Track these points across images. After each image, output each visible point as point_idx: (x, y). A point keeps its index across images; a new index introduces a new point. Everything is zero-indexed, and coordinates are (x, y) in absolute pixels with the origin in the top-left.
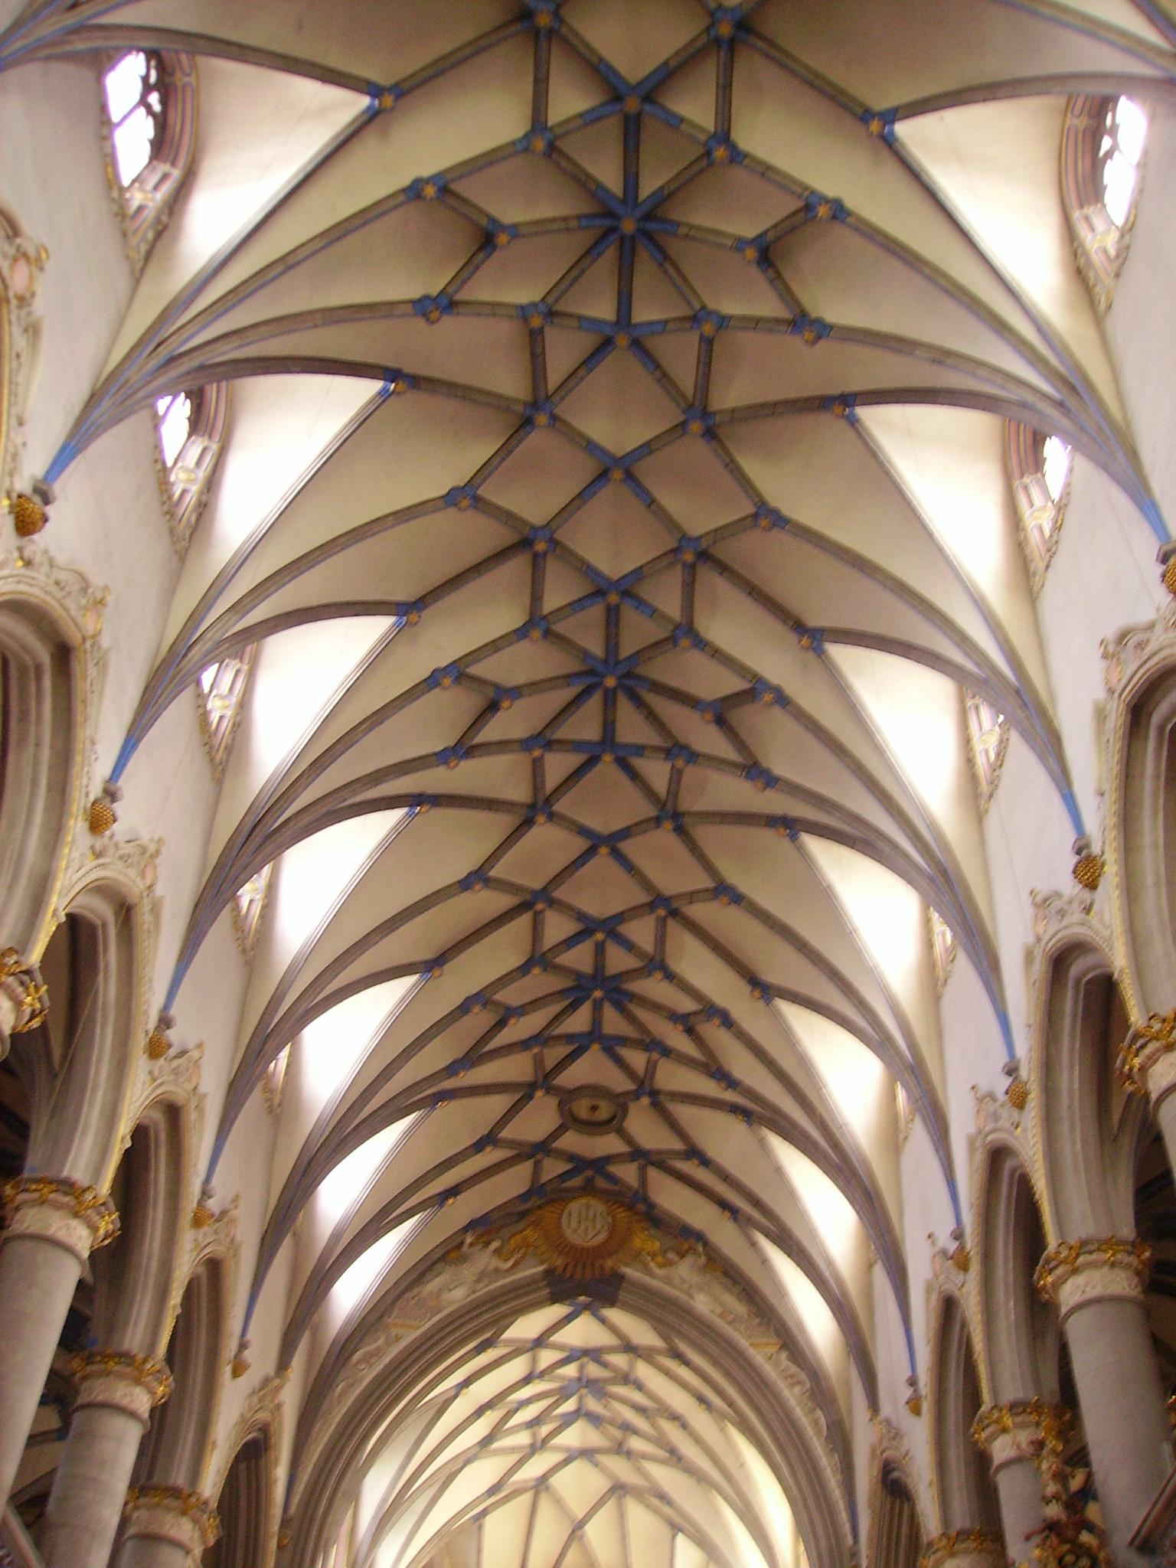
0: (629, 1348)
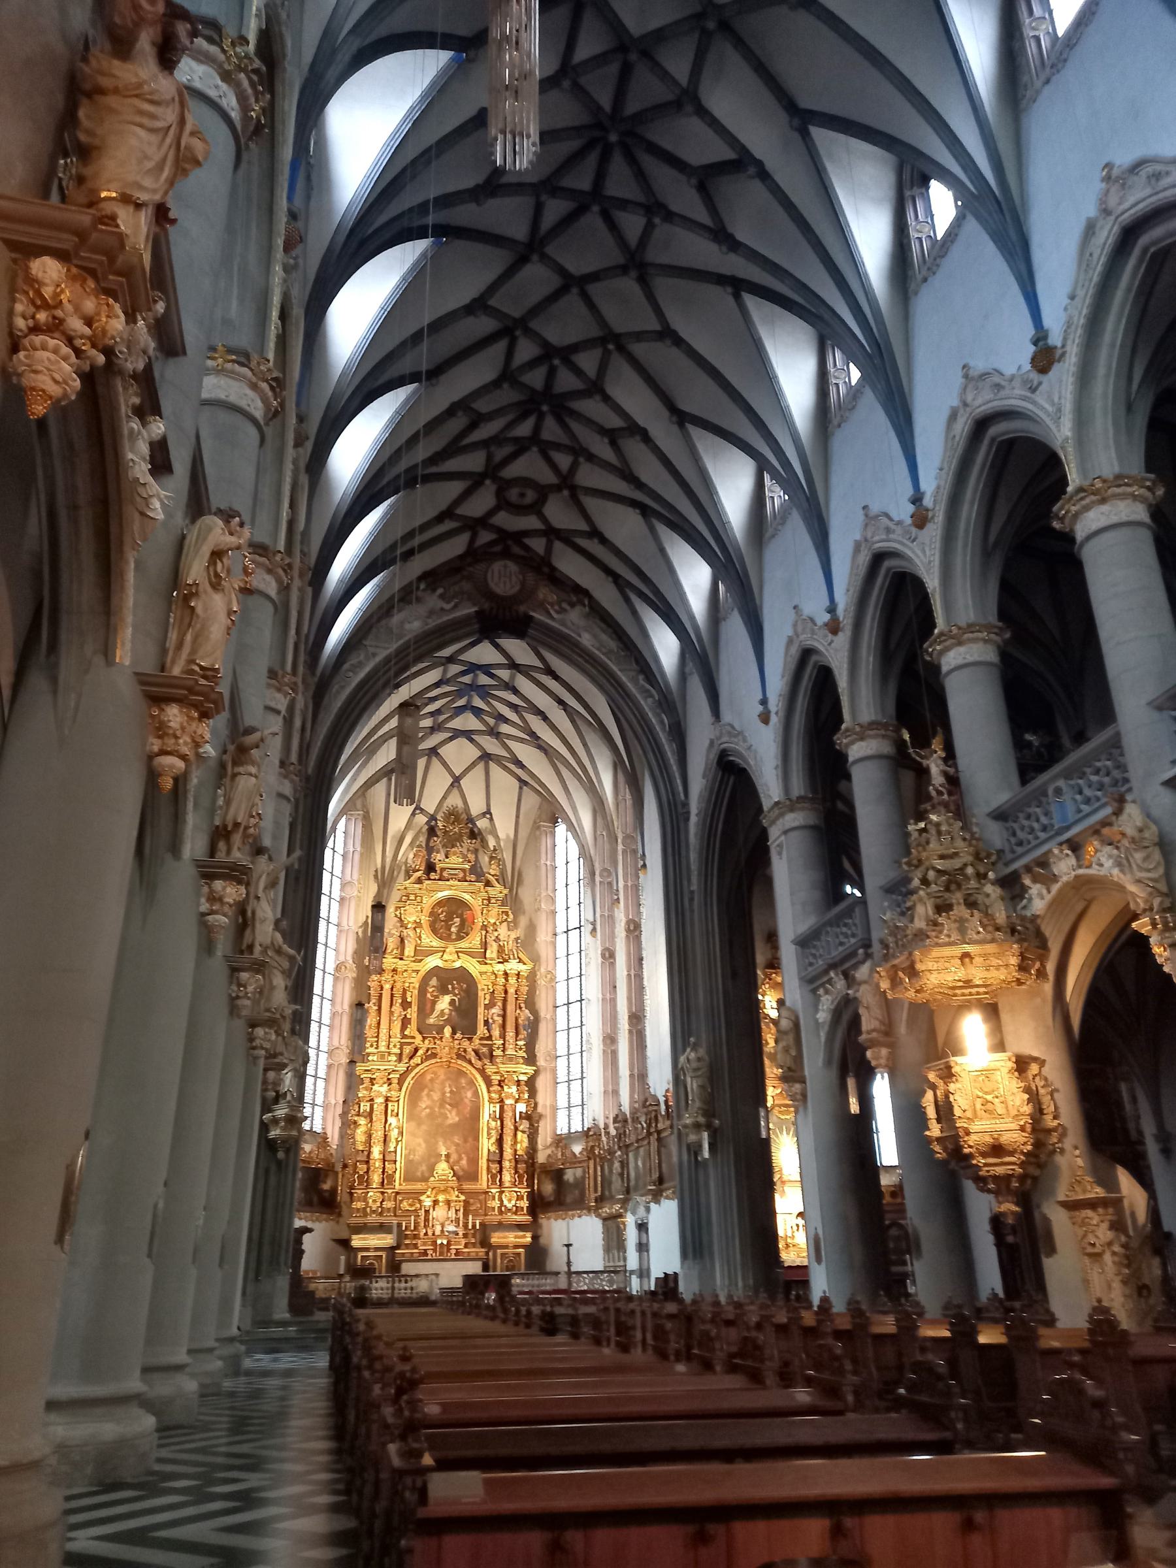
0: (514, 666)
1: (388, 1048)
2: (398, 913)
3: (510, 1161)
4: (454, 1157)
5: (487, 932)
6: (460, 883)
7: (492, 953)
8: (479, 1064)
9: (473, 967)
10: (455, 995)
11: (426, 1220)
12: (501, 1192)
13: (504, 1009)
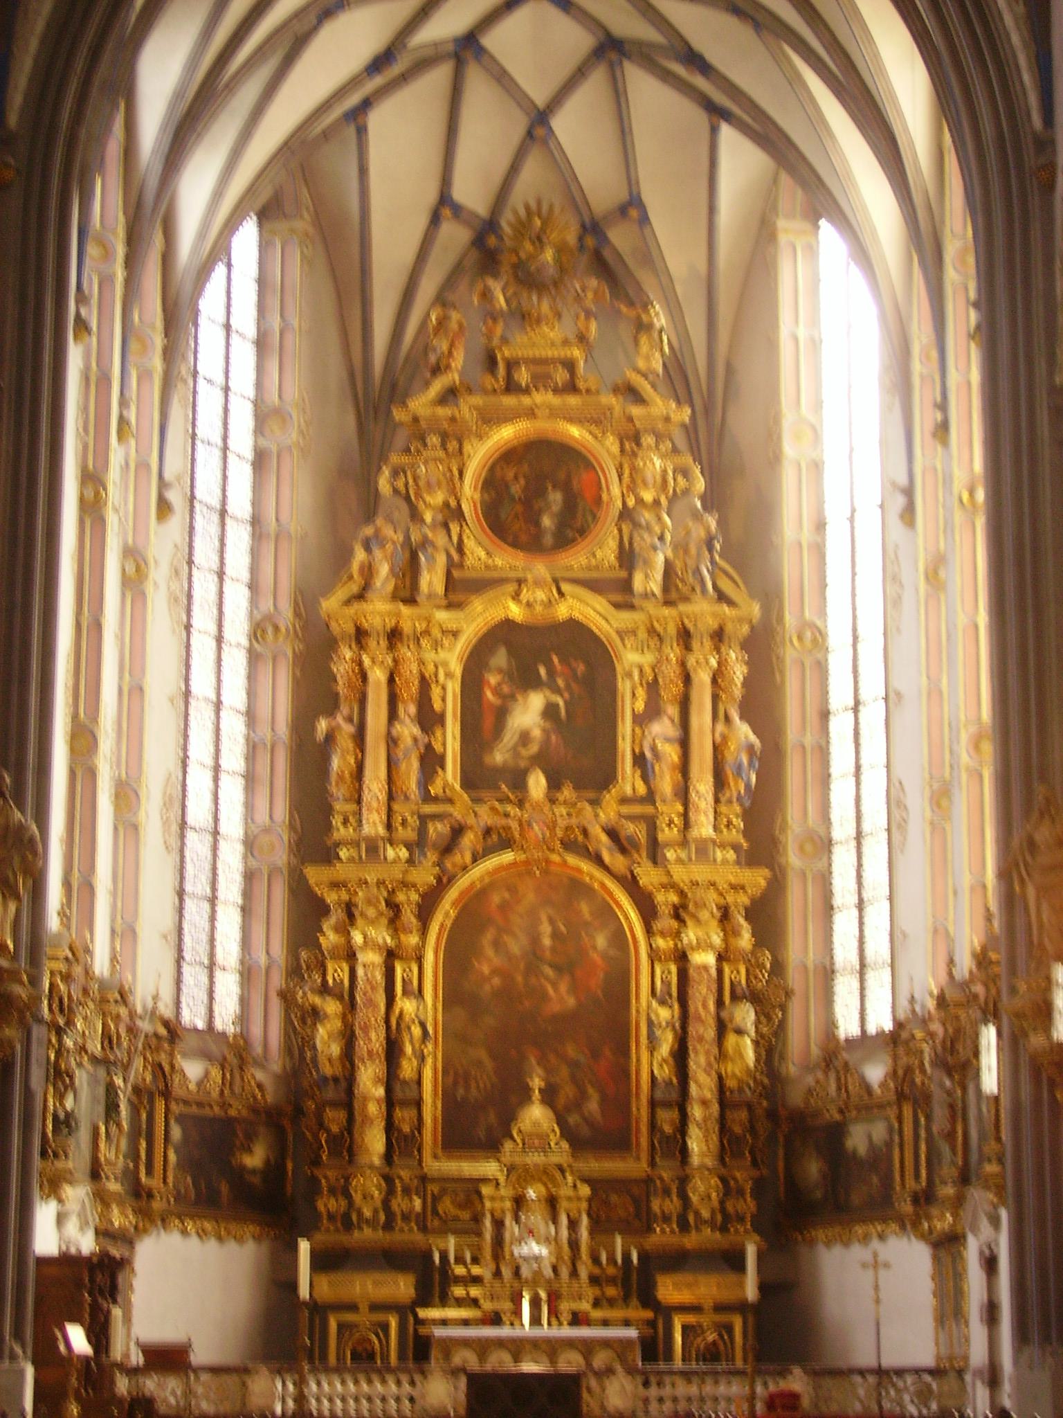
1: (389, 826)
3: (704, 1103)
4: (567, 1092)
5: (636, 525)
6: (555, 400)
7: (648, 581)
10: (558, 691)
11: (498, 1242)
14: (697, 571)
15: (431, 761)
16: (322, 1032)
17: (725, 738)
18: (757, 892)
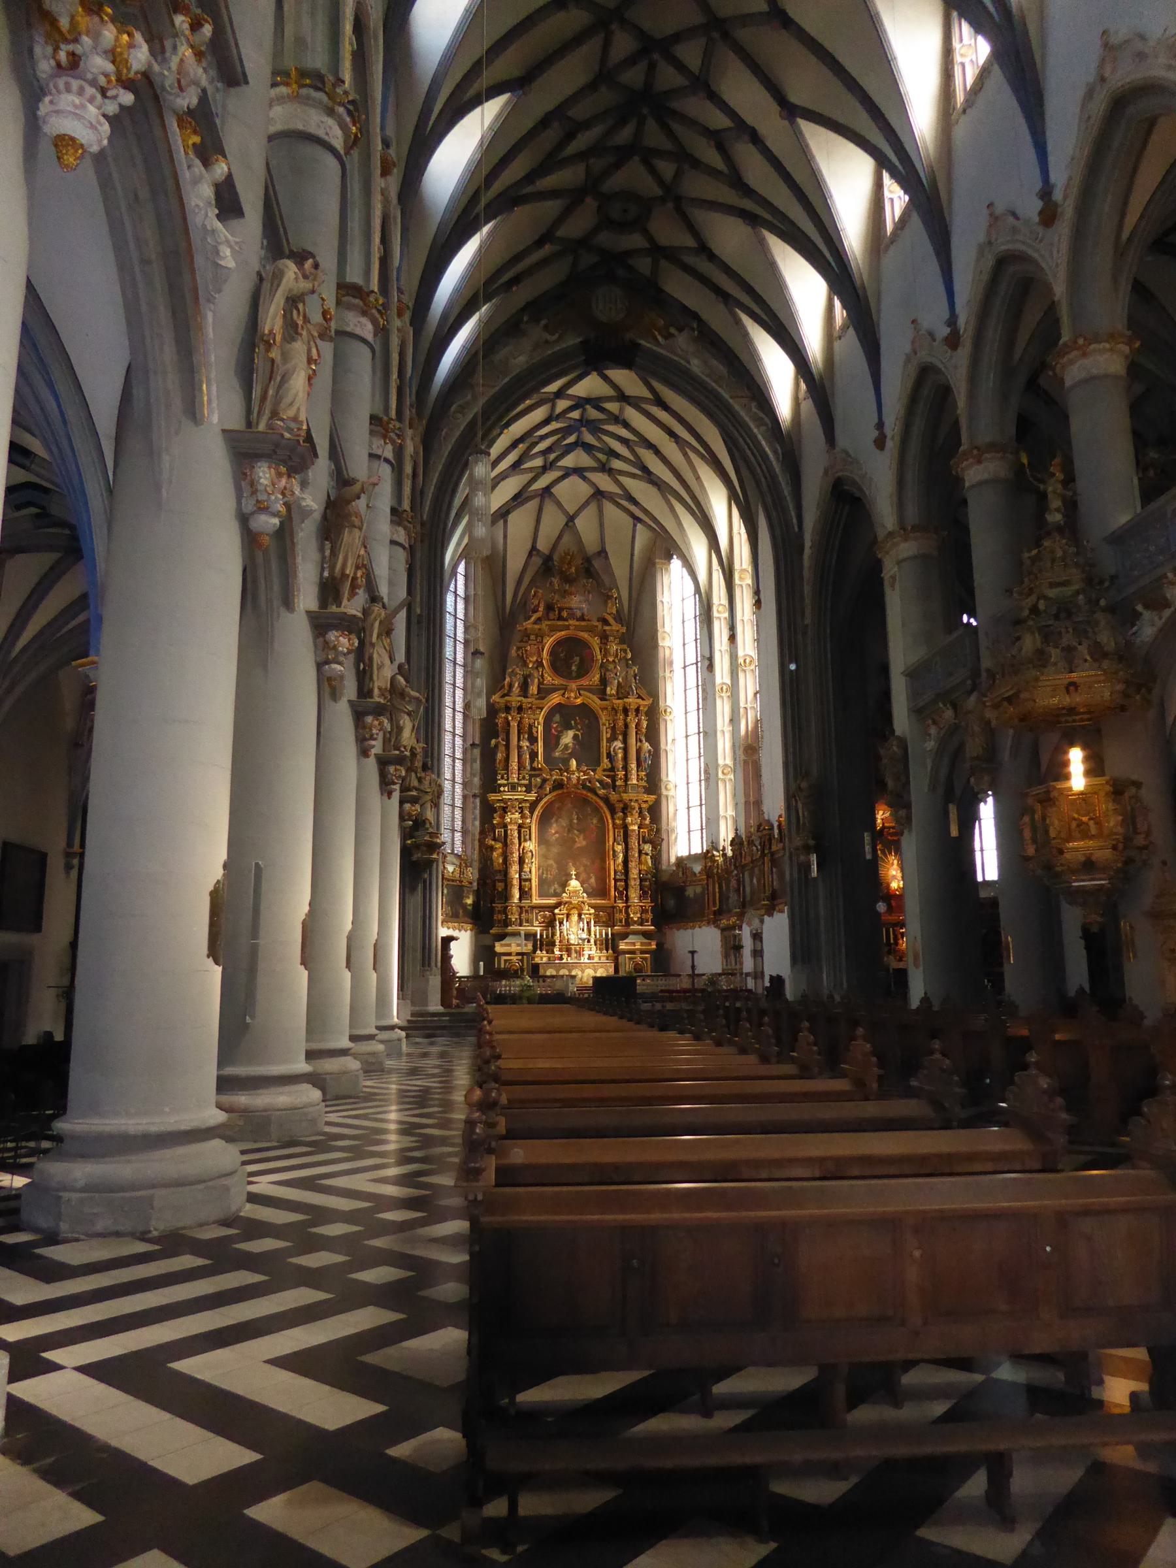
0: (622, 397)
1: (518, 779)
2: (520, 653)
5: (607, 670)
6: (577, 623)
7: (611, 690)
8: (602, 792)
9: (595, 702)
10: (578, 730)
12: (627, 907)
13: (625, 741)
14: (631, 687)
15: (534, 755)
16: (495, 854)
17: (640, 747)
18: (651, 803)
